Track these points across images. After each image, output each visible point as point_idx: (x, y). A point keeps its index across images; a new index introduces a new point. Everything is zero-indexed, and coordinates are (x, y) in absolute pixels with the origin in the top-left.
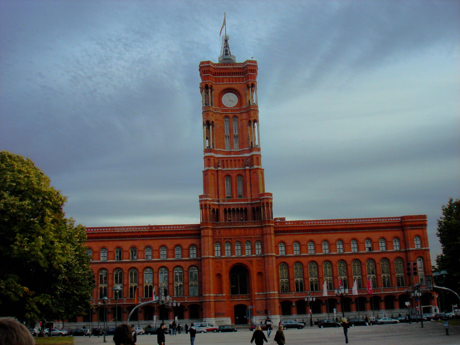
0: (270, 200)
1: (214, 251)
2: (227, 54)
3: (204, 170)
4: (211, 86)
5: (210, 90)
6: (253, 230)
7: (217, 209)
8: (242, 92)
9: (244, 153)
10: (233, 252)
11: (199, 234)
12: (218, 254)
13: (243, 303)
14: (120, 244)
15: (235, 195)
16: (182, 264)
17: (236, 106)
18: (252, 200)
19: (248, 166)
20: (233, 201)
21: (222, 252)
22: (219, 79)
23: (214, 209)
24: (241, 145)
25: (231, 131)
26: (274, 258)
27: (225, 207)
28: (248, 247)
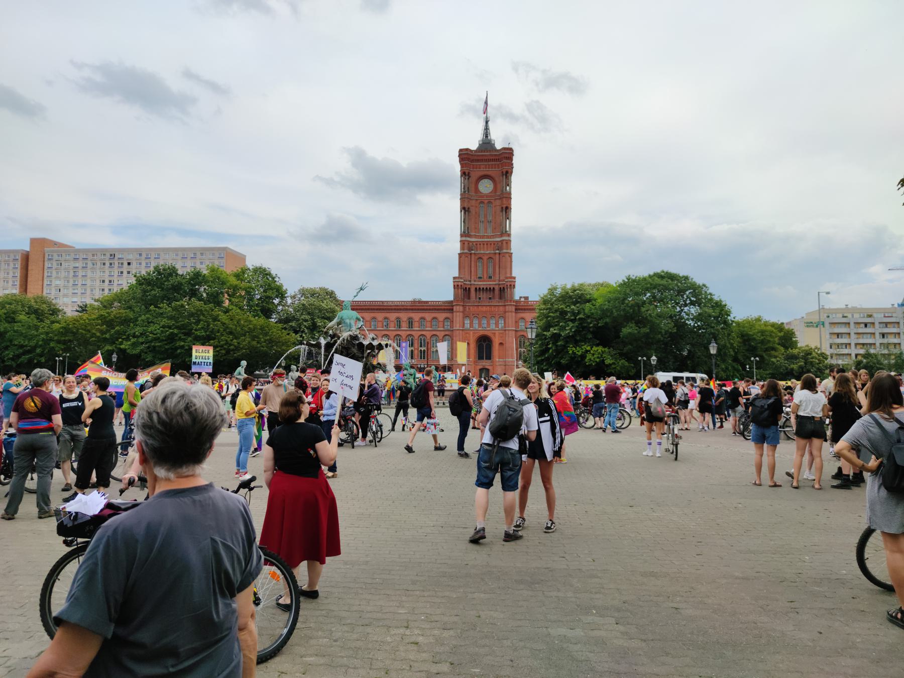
0: (513, 284)
1: (464, 324)
2: (487, 137)
3: (459, 252)
4: (469, 173)
5: (467, 177)
6: (497, 307)
7: (469, 288)
8: (497, 179)
9: (496, 237)
10: (480, 325)
11: (452, 309)
12: (467, 326)
13: (487, 367)
14: (387, 315)
15: (485, 277)
16: (437, 333)
17: (491, 192)
18: (499, 281)
19: (498, 250)
20: (483, 281)
21: (471, 324)
22: (477, 165)
23: (466, 288)
24: (494, 229)
25: (486, 216)
26: (514, 332)
27: (475, 287)
28: (493, 322)
